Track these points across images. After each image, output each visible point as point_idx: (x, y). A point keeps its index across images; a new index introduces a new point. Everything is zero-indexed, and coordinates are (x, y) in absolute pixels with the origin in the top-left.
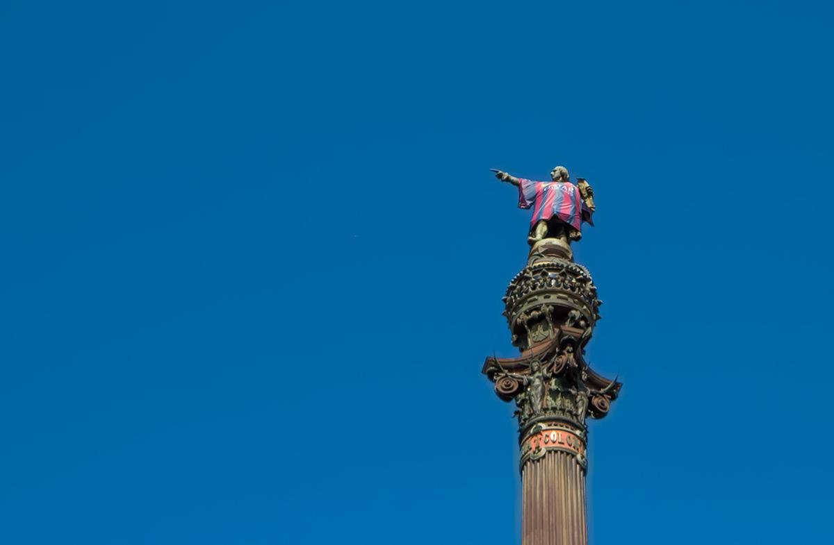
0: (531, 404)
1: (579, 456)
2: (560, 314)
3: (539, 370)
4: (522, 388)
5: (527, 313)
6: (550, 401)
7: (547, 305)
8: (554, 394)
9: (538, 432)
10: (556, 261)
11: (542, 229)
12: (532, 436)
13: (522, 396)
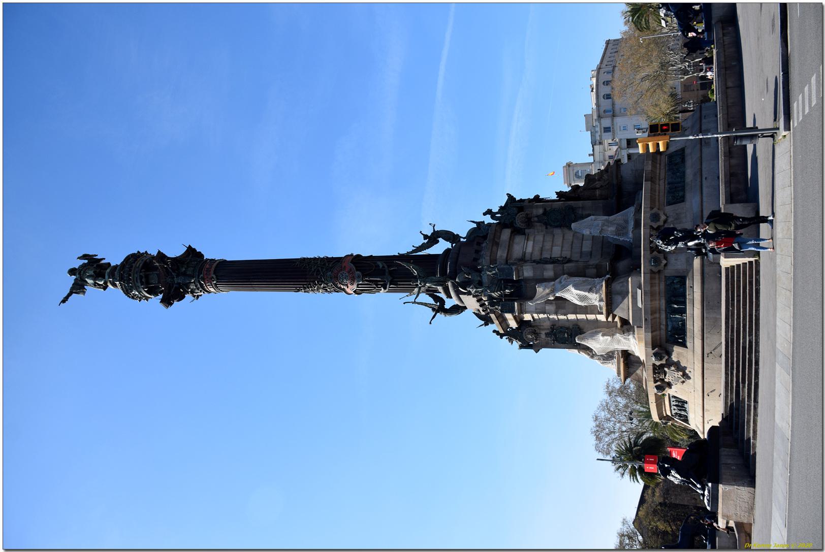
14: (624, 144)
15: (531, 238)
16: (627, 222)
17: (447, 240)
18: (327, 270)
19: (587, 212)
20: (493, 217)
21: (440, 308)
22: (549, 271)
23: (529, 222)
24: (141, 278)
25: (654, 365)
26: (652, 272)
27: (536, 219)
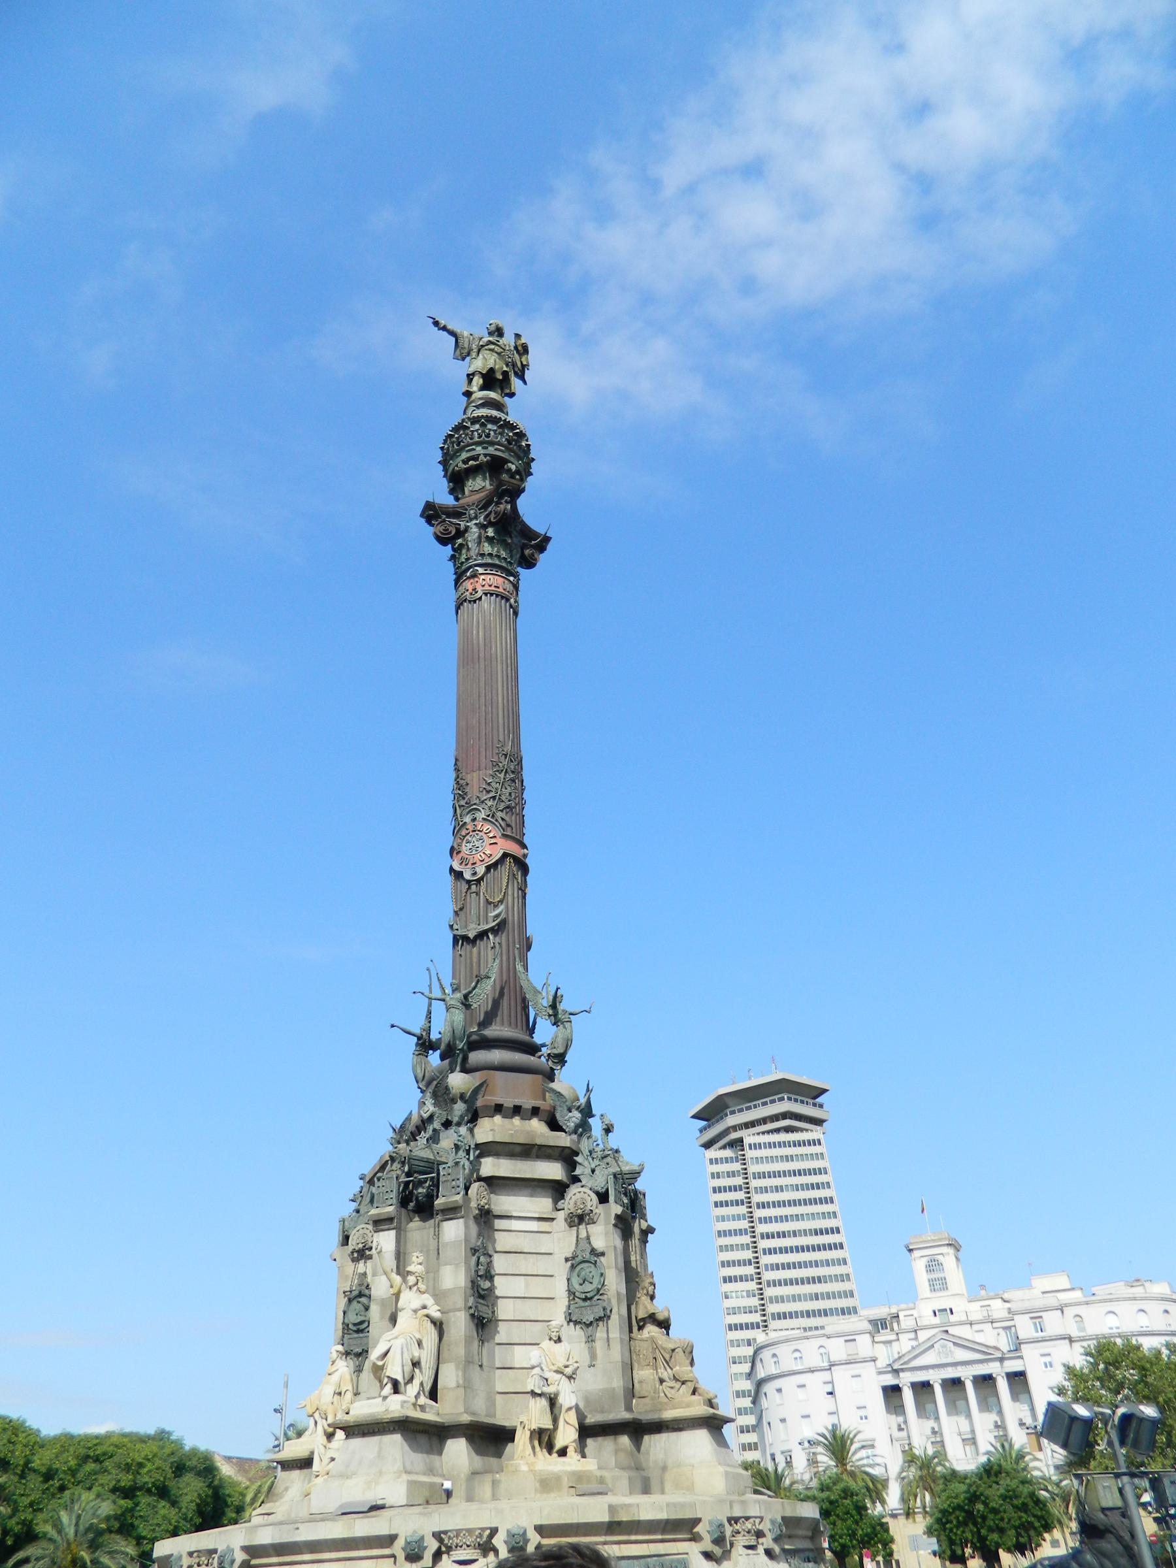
0: (468, 549)
1: (512, 601)
2: (495, 466)
3: (476, 518)
4: (460, 533)
5: (465, 462)
6: (487, 548)
7: (486, 455)
8: (490, 540)
9: (474, 576)
10: (495, 413)
11: (478, 381)
12: (468, 578)
13: (460, 541)
14: (1013, 1366)
15: (544, 1226)
16: (563, 1452)
18: (490, 808)
19: (599, 1352)
22: (454, 1278)
23: (579, 1219)
27: (583, 1234)
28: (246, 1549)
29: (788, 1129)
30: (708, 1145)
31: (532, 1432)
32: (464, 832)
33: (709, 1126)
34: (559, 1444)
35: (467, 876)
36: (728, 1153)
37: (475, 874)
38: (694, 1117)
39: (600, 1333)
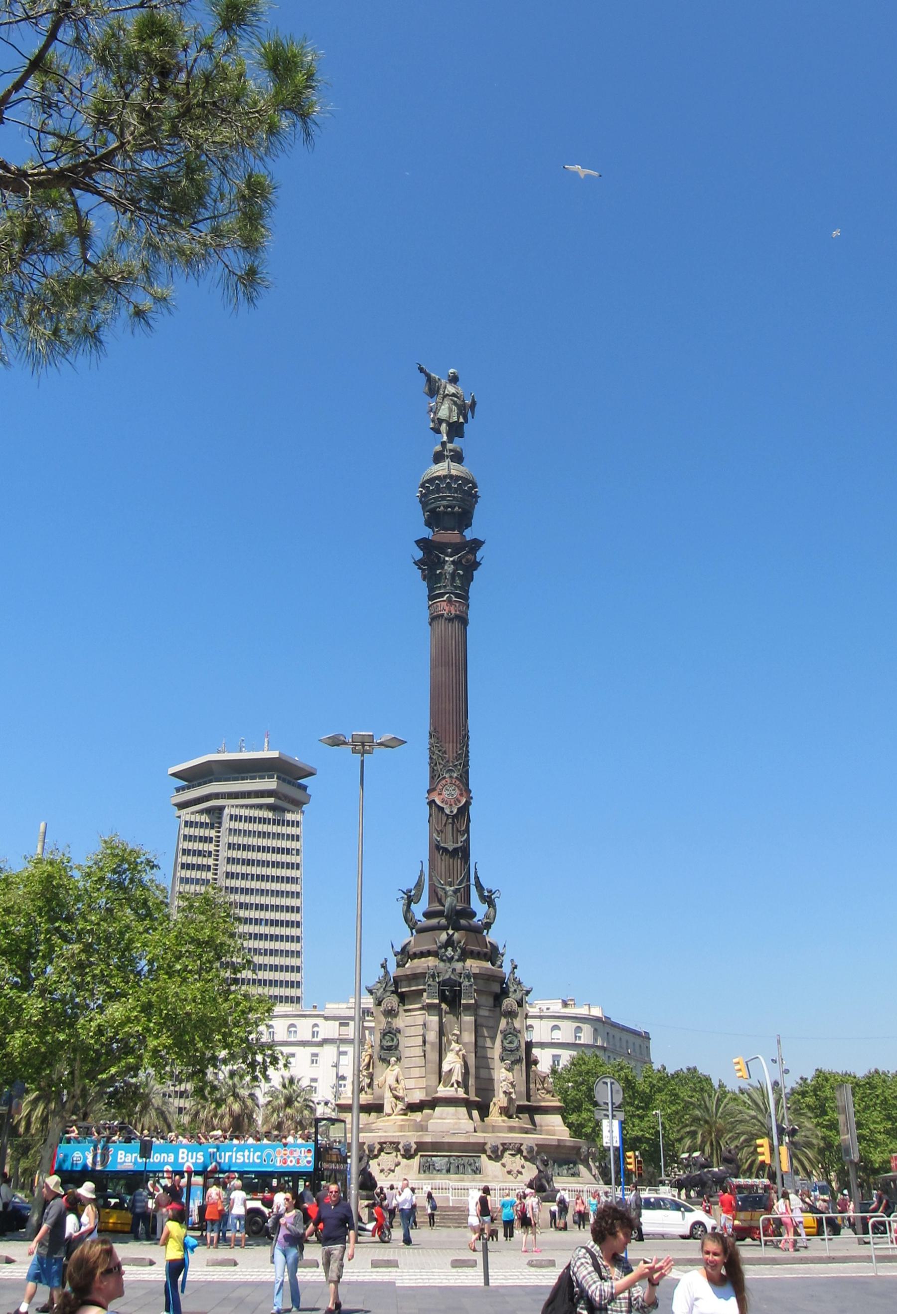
5: (446, 507)
17: (487, 916)
20: (513, 972)
21: (410, 899)
22: (469, 1037)
24: (453, 507)
25: (399, 1143)
26: (485, 1144)
28: (416, 1143)
29: (270, 807)
30: (182, 806)
31: (500, 1108)
32: (444, 782)
33: (189, 788)
34: (511, 1112)
35: (447, 811)
36: (205, 818)
37: (452, 812)
38: (173, 775)
39: (517, 1067)
